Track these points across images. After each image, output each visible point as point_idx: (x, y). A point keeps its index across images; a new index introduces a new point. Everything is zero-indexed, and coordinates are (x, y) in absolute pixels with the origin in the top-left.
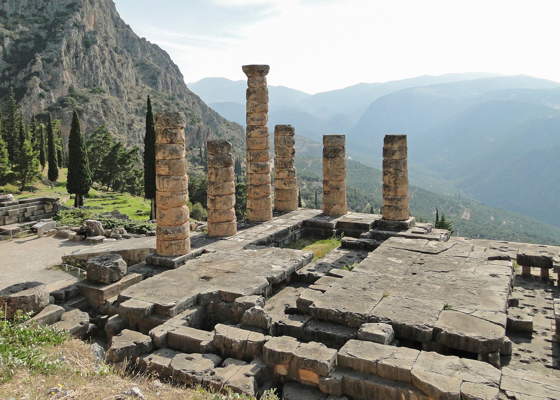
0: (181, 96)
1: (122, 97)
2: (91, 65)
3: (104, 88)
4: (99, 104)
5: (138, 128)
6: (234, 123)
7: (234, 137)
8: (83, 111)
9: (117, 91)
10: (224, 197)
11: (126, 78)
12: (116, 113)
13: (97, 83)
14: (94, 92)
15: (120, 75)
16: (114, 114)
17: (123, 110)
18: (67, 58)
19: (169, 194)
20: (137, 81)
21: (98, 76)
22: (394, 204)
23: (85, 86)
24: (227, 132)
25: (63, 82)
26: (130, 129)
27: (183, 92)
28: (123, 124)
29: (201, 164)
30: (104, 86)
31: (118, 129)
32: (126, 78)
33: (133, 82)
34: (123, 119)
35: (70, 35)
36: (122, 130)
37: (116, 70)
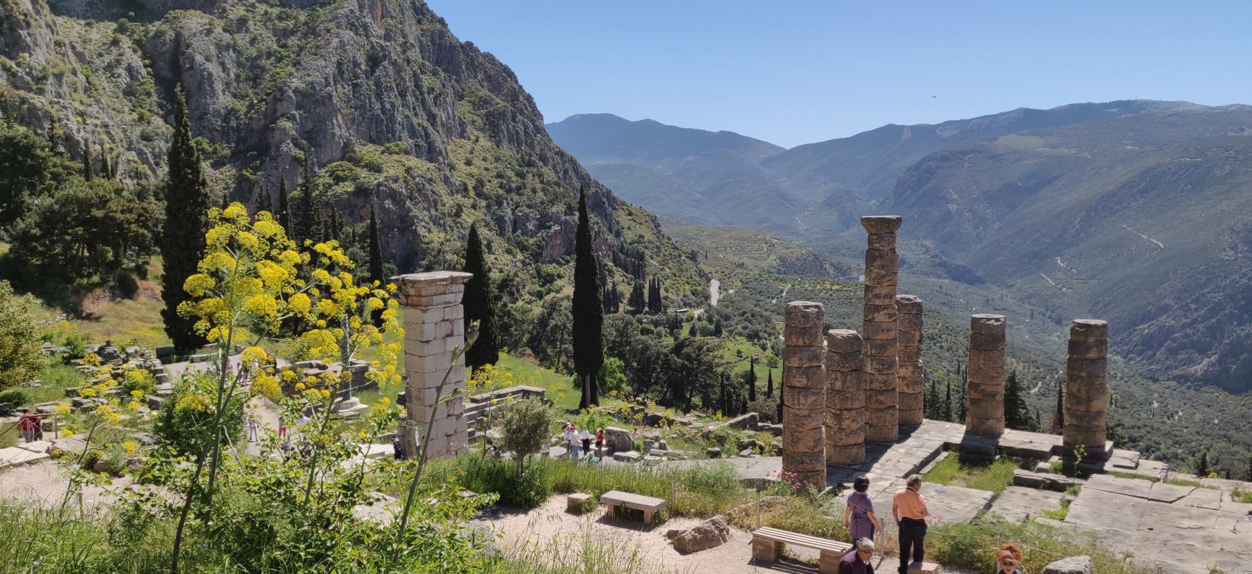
7: (641, 236)
10: (854, 412)
15: (432, 118)
19: (806, 413)
22: (1085, 424)
23: (372, 141)
25: (334, 135)
37: (425, 109)
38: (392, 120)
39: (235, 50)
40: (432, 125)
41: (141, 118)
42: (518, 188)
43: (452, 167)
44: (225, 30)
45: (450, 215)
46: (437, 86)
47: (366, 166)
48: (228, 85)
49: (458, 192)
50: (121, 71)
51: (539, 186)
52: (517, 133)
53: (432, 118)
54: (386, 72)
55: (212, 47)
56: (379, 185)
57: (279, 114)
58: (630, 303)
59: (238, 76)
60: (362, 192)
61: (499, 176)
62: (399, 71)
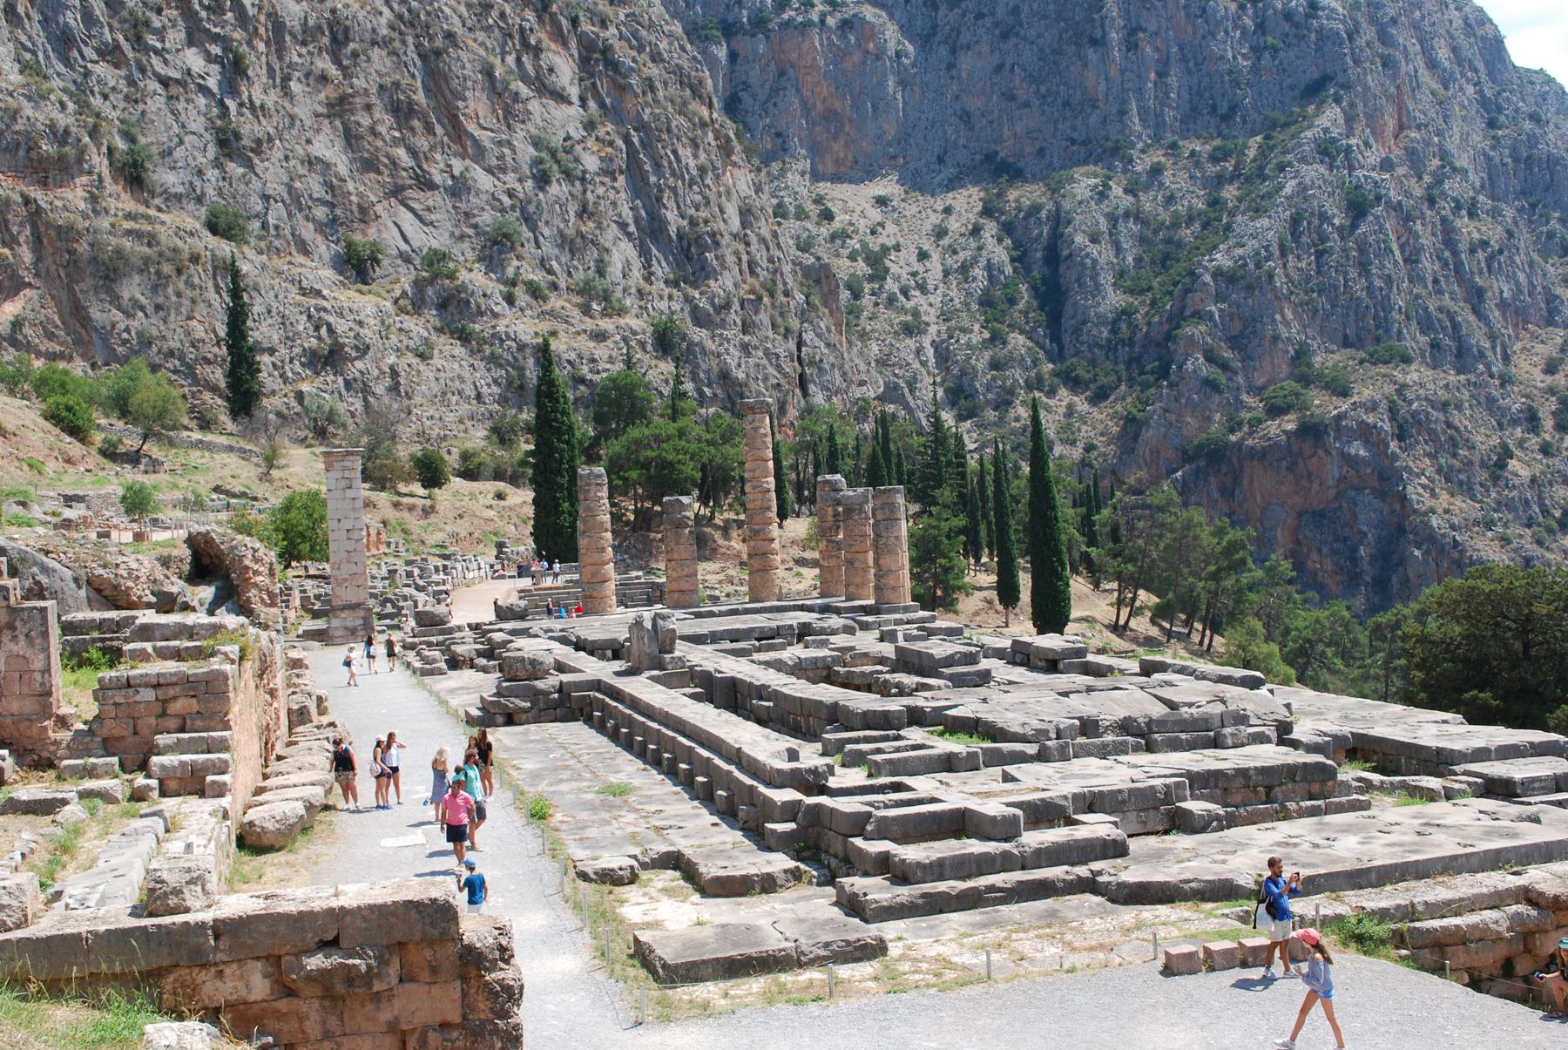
11: (1503, 305)
13: (1387, 331)
15: (1476, 297)
16: (1432, 432)
23: (1346, 343)
25: (1276, 339)
30: (1415, 340)
32: (1503, 305)
38: (1386, 305)
39: (1137, 218)
40: (1475, 311)
41: (993, 339)
43: (1505, 380)
45: (1483, 464)
46: (1495, 235)
47: (1327, 387)
48: (1121, 274)
49: (1515, 422)
50: (978, 272)
53: (1476, 297)
54: (1381, 226)
55: (1102, 220)
56: (1340, 417)
57: (1187, 313)
59: (1138, 260)
60: (1312, 431)
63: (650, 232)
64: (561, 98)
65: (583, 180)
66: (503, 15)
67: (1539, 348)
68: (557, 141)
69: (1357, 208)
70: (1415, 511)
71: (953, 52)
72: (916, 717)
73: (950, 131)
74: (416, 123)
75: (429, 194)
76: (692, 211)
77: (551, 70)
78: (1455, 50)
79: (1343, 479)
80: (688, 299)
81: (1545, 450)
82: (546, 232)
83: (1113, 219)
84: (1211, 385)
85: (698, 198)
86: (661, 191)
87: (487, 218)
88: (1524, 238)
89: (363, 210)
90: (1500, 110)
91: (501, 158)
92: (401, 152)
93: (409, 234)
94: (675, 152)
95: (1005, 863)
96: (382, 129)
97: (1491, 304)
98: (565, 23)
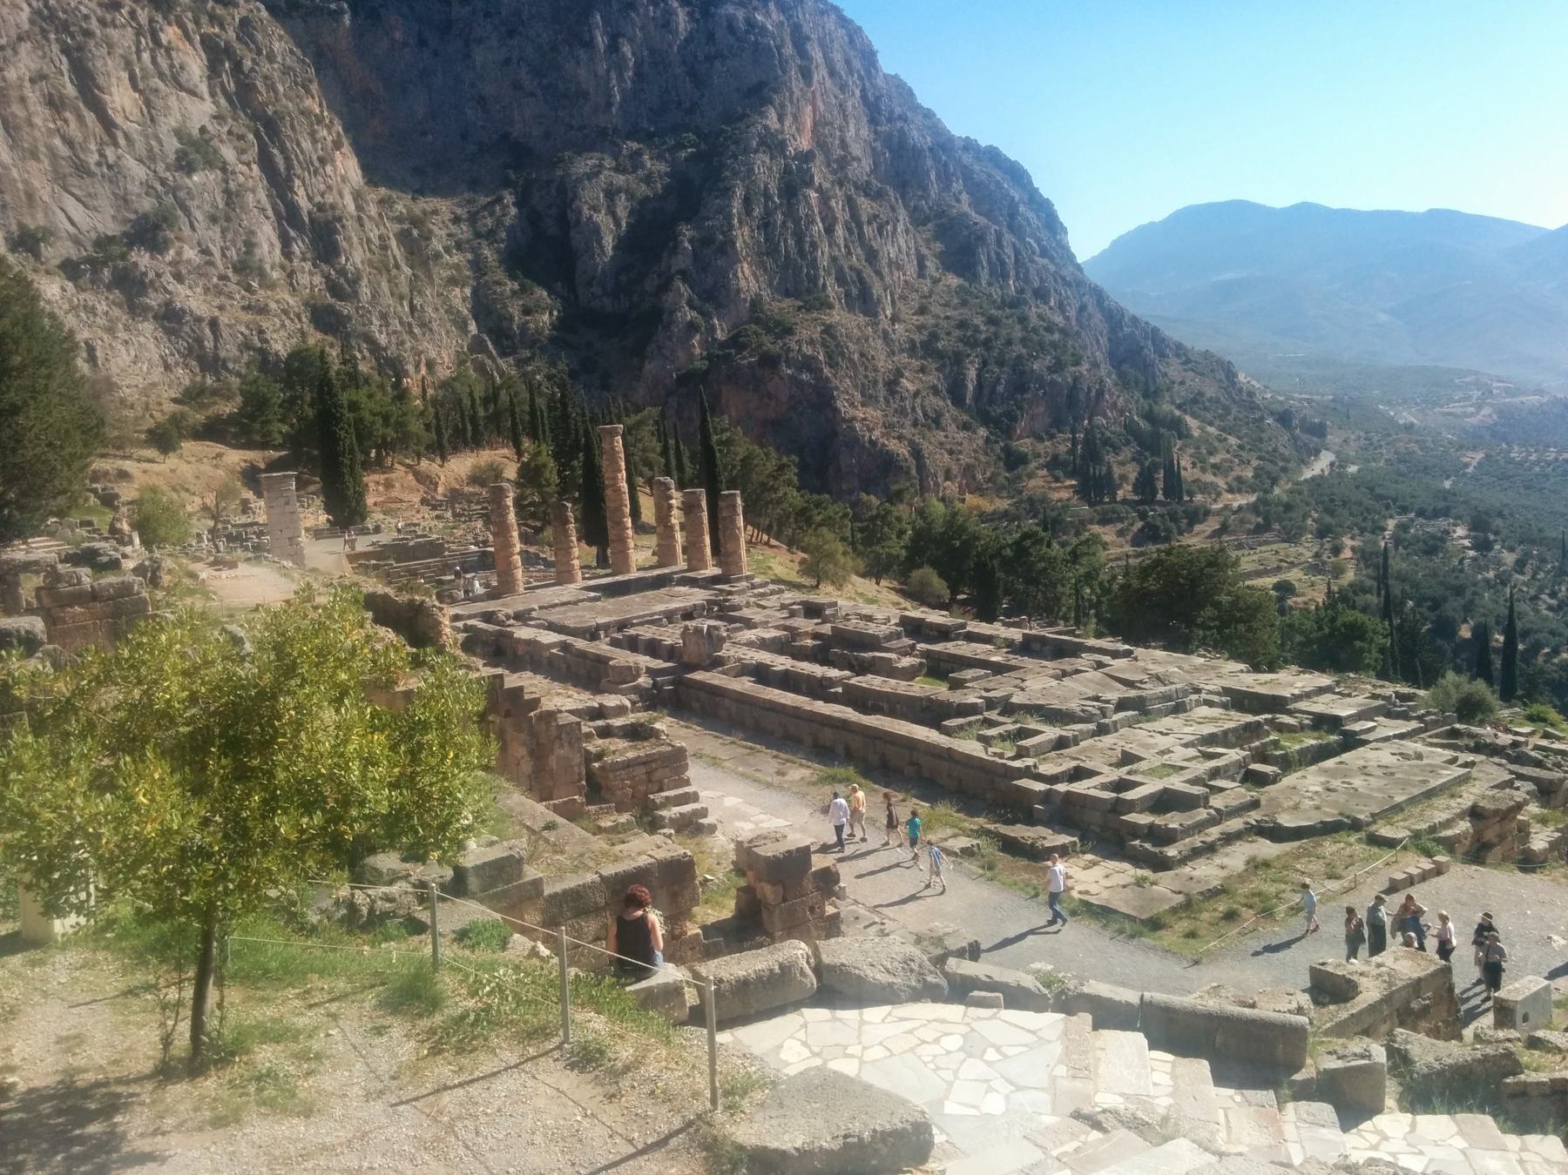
0: (1041, 295)
1: (875, 315)
2: (800, 240)
3: (832, 294)
4: (817, 336)
5: (912, 388)
6: (1207, 355)
7: (1201, 394)
8: (779, 356)
9: (863, 301)
12: (856, 356)
13: (816, 285)
14: (808, 308)
15: (872, 256)
16: (851, 360)
17: (877, 347)
18: (746, 230)
20: (921, 266)
21: (816, 268)
23: (787, 294)
24: (1182, 383)
25: (738, 291)
26: (892, 392)
27: (1050, 284)
28: (875, 382)
29: (1070, 476)
30: (833, 290)
31: (863, 395)
33: (911, 269)
34: (876, 370)
35: (750, 171)
36: (871, 397)
38: (814, 264)
39: (627, 192)
41: (523, 289)
42: (987, 344)
44: (617, 170)
51: (1018, 333)
52: (1003, 263)
57: (673, 270)
58: (1135, 491)
60: (770, 362)
61: (962, 325)
62: (825, 198)
63: (288, 216)
64: (193, 93)
65: (224, 170)
66: (133, 14)
67: (914, 296)
68: (195, 132)
69: (792, 186)
70: (844, 420)
71: (467, 44)
72: (990, 704)
73: (469, 112)
74: (68, 115)
75: (88, 180)
76: (318, 199)
77: (182, 68)
78: (848, 62)
79: (792, 397)
80: (327, 277)
81: (923, 370)
82: (198, 215)
83: (611, 194)
84: (692, 327)
85: (322, 187)
86: (289, 179)
87: (147, 205)
88: (903, 215)
89: (30, 196)
90: (879, 111)
91: (150, 150)
92: (57, 142)
93: (76, 219)
94: (298, 145)
95: (1212, 822)
96: (38, 121)
97: (884, 262)
98: (190, 26)
